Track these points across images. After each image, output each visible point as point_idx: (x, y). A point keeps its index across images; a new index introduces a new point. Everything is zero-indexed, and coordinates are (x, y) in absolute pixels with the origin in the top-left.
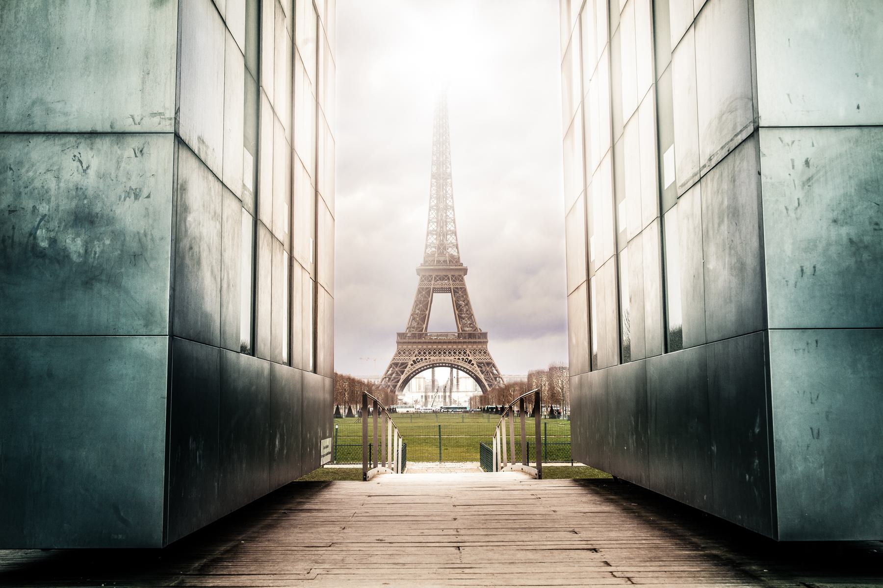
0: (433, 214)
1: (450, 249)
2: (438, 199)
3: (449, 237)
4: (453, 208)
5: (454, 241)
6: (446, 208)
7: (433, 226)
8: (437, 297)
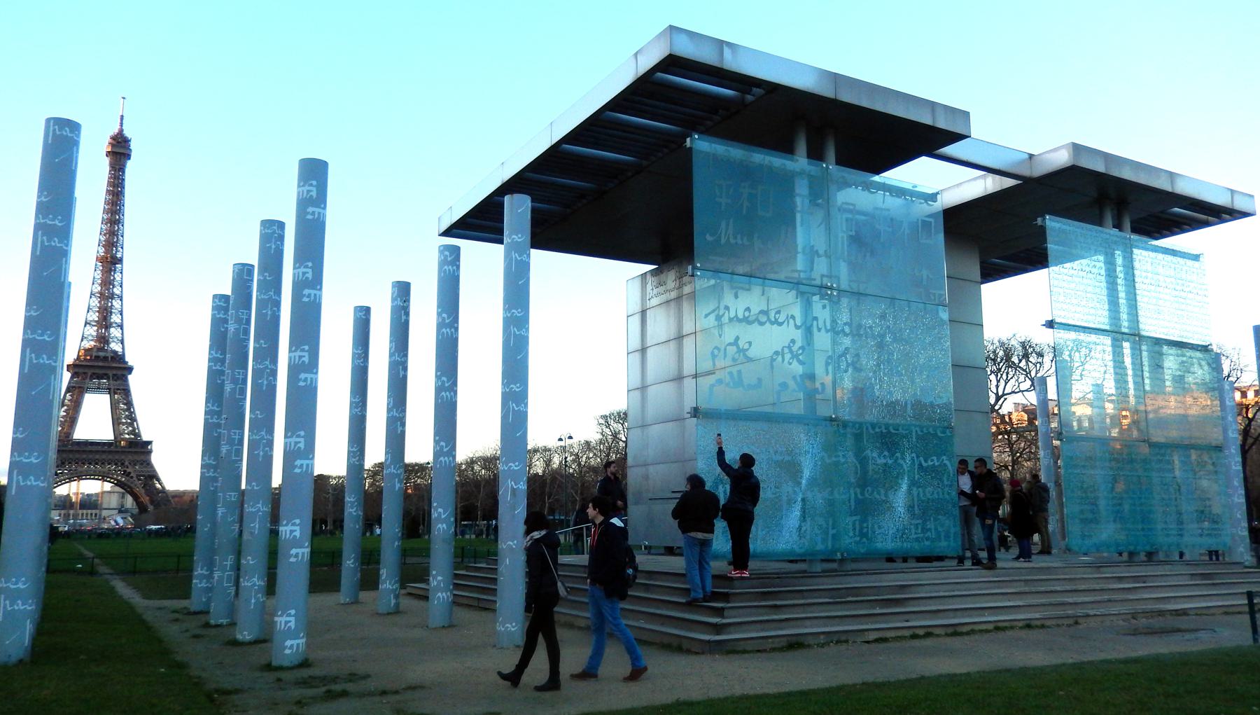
0: (95, 302)
3: (112, 330)
4: (121, 298)
5: (119, 335)
6: (112, 296)
7: (94, 317)
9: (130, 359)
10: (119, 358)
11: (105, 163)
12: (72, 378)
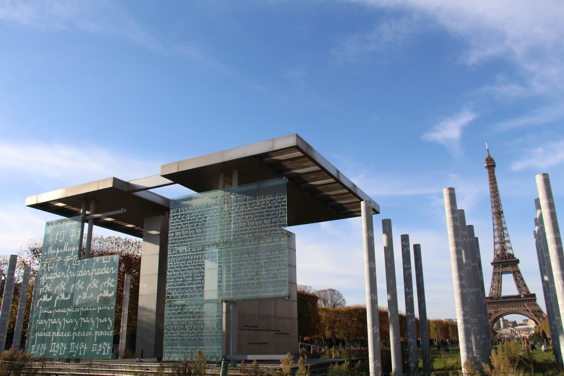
2: (498, 224)
7: (497, 239)
8: (504, 277)
9: (517, 256)
10: (513, 256)
11: (486, 171)
12: (494, 268)
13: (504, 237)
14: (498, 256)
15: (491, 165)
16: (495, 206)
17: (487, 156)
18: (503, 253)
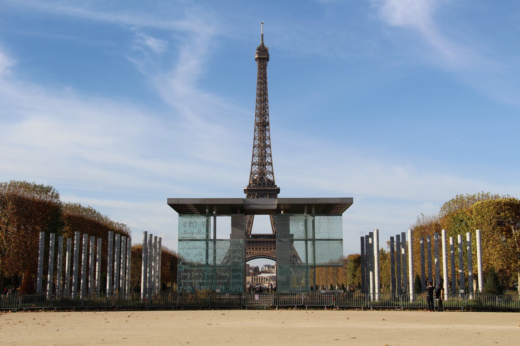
1: (268, 175)
2: (260, 139)
3: (267, 166)
7: (256, 159)
9: (278, 184)
10: (272, 183)
11: (255, 65)
13: (265, 157)
14: (254, 181)
15: (263, 56)
16: (260, 114)
17: (260, 43)
18: (261, 179)
